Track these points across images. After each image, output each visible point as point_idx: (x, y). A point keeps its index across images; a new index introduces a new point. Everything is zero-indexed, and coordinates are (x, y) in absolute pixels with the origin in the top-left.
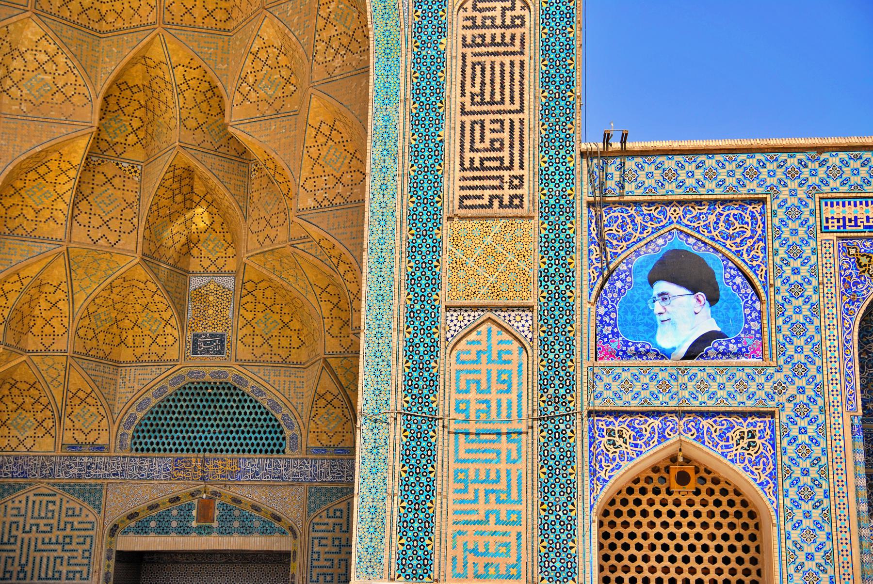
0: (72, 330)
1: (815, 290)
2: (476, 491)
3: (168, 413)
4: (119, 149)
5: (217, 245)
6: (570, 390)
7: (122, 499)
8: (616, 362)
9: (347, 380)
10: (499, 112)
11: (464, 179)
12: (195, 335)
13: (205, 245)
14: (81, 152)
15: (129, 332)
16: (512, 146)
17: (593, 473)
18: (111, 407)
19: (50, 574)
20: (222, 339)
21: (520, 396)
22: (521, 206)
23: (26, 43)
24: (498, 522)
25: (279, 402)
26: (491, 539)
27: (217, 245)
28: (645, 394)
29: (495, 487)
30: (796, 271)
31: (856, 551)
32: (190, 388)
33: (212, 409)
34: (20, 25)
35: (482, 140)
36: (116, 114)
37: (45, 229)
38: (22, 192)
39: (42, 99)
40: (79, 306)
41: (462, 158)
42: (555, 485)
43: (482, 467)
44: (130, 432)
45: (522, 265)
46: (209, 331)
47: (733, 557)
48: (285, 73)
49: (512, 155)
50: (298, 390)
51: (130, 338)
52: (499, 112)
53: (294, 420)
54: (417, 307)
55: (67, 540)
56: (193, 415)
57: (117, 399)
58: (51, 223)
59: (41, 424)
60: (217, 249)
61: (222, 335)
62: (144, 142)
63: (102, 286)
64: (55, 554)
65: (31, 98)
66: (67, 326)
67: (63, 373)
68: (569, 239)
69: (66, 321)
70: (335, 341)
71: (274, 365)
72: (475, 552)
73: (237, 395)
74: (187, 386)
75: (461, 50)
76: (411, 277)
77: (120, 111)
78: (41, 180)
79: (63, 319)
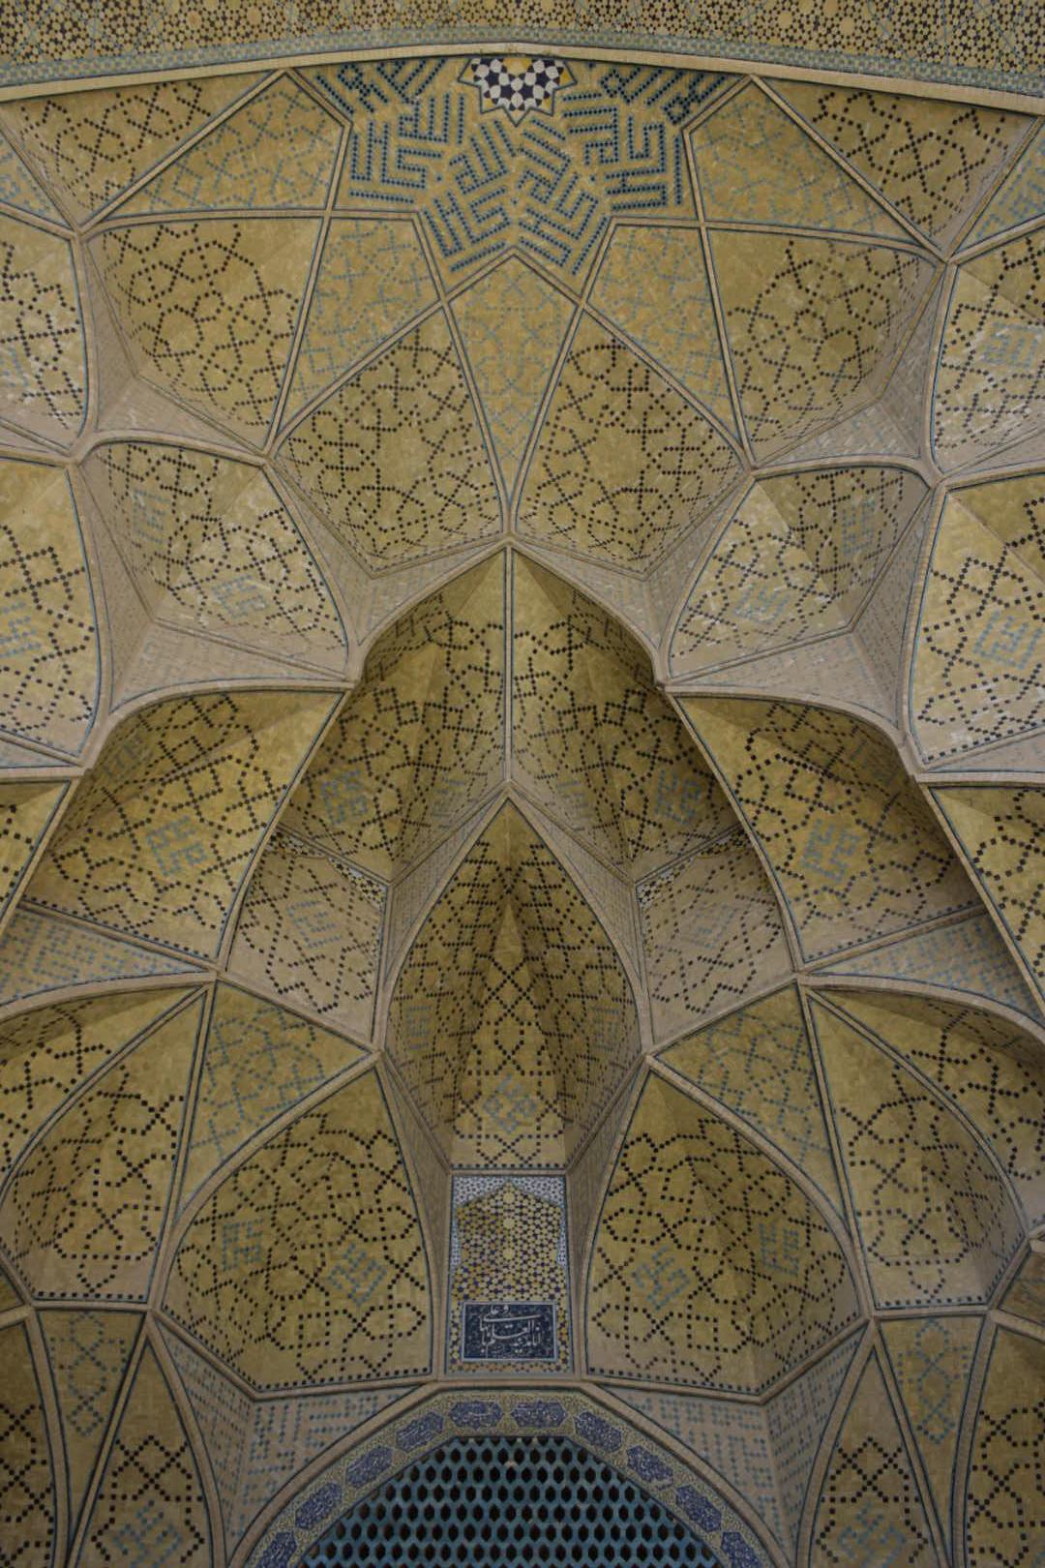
0: (168, 1247)
3: (389, 1533)
4: (346, 845)
5: (518, 1107)
9: (925, 1400)
12: (470, 1309)
13: (492, 1105)
14: (302, 749)
15: (290, 1306)
18: (226, 1511)
20: (543, 1317)
23: (240, 516)
25: (712, 1497)
27: (518, 1107)
32: (456, 1456)
33: (518, 1520)
34: (240, 474)
36: (353, 768)
37: (172, 928)
38: (139, 833)
39: (243, 619)
40: (194, 1187)
46: (509, 1300)
50: (755, 1462)
51: (292, 1323)
53: (758, 1551)
56: (461, 1540)
57: (241, 1493)
58: (190, 920)
60: (520, 1117)
61: (543, 1308)
62: (394, 848)
63: (266, 1134)
65: (224, 612)
66: (156, 1233)
67: (113, 1383)
69: (155, 1220)
73: (590, 1476)
74: (448, 1450)
77: (362, 764)
78: (190, 811)
79: (151, 1213)
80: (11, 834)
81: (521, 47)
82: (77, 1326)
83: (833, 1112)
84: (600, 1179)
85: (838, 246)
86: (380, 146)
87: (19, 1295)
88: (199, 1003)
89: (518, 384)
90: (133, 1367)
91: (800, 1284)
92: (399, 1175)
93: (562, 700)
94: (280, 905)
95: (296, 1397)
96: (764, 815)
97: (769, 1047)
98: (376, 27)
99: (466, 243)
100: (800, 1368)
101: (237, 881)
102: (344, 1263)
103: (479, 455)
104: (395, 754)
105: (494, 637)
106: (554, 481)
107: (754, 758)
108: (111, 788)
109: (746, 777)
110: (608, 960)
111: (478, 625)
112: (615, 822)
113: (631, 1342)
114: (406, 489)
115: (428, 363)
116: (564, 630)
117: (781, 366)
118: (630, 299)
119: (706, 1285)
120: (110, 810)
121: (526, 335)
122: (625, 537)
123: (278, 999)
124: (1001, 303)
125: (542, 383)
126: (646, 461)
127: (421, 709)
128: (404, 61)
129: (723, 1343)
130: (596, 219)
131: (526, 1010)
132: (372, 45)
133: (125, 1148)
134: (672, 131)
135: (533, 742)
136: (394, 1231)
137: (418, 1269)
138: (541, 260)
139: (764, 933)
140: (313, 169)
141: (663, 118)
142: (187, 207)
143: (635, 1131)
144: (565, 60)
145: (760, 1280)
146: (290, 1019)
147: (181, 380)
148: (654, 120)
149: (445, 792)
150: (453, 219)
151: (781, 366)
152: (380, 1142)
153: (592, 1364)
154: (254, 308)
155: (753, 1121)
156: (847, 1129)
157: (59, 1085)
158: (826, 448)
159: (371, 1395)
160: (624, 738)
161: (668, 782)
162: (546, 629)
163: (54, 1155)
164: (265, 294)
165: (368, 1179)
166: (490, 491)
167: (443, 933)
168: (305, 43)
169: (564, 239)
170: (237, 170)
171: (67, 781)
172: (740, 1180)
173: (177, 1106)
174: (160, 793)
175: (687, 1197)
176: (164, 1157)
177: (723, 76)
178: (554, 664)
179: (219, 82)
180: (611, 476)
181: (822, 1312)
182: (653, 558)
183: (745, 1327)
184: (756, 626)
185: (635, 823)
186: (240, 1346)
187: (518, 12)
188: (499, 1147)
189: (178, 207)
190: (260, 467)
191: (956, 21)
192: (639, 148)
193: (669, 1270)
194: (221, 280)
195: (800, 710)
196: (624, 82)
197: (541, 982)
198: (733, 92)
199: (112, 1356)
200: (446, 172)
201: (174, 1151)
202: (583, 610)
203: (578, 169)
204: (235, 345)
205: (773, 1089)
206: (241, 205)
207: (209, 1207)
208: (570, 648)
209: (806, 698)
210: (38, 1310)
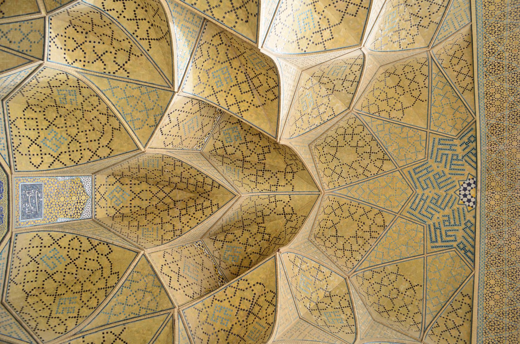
13: (118, 189)
14: (256, 123)
34: (347, 101)
36: (243, 138)
38: (227, 64)
39: (300, 102)
40: (92, 80)
46: (44, 200)
51: (34, 115)
60: (114, 200)
62: (214, 152)
63: (113, 108)
66: (75, 65)
67: (12, 46)
77: (244, 141)
78: (235, 82)
80: (237, 20)
81: (479, 193)
82: (37, 33)
83: (124, 324)
84: (93, 234)
85: (421, 302)
86: (449, 148)
87: (52, 11)
88: (166, 85)
89: (371, 194)
90: (20, 54)
91: (53, 315)
92: (95, 157)
93: (267, 212)
94: (198, 113)
95: (4, 117)
96: (234, 290)
97: (148, 298)
98: (487, 148)
99: (417, 176)
100: (19, 318)
101: (209, 99)
102: (59, 136)
103: (348, 181)
104: (248, 153)
107: (254, 285)
108: (245, 55)
109: (247, 282)
110: (177, 233)
111: (293, 182)
112: (223, 231)
113: (28, 249)
114: (336, 156)
115: (379, 163)
116: (291, 212)
117: (381, 284)
118: (400, 231)
119: (50, 276)
120: (236, 53)
121: (388, 196)
122: (321, 231)
123: (166, 114)
126: (347, 238)
127: (263, 162)
128: (476, 157)
129: (26, 284)
130: (425, 219)
131: (155, 201)
132: (482, 147)
133: (108, 54)
134: (455, 244)
135: (253, 202)
136: (72, 155)
137: (57, 165)
138: (412, 201)
139: (190, 292)
140: (443, 126)
141: (459, 241)
142: (433, 85)
143: (113, 247)
144: (476, 208)
145: (53, 298)
146: (158, 118)
147: (377, 81)
148: (458, 238)
149: (235, 171)
152: (109, 151)
153: (19, 235)
154: (398, 106)
155: (119, 293)
156: (117, 330)
157: (136, 31)
158: (358, 303)
159: (6, 148)
160: (253, 234)
161: (238, 250)
162: (292, 206)
163: (107, 27)
164: (403, 109)
165: (94, 146)
166: (337, 186)
167: (186, 172)
168: (483, 125)
169: (419, 208)
170: (444, 102)
171: (257, 42)
172: (94, 289)
173: (125, 74)
174: (242, 72)
175: (86, 268)
176: (105, 69)
177: (474, 261)
178: (279, 209)
179: (473, 97)
180: (341, 226)
181: (43, 325)
182: (316, 242)
183: (33, 293)
184: (299, 282)
185: (222, 238)
186: (26, 96)
187: (490, 193)
188: (102, 193)
189: (433, 82)
190: (349, 108)
191: (496, 339)
192: (449, 233)
193: (56, 262)
194: (408, 95)
195: (274, 303)
196: (469, 228)
197: (166, 207)
198: (469, 265)
199: (24, 46)
200: (440, 170)
201: (107, 73)
202: (299, 219)
203: (441, 213)
204: (387, 99)
205: (132, 300)
206: (432, 102)
207: (84, 85)
208: (285, 214)
209: (279, 305)
210: (45, 18)
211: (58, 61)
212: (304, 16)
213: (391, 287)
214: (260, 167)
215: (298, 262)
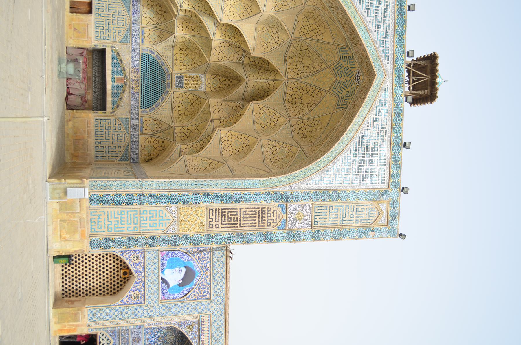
1: (182, 314)
2: (118, 218)
6: (151, 246)
7: (124, 51)
8: (160, 257)
10: (240, 220)
11: (219, 210)
16: (229, 224)
17: (125, 252)
19: (97, 25)
20: (181, 86)
21: (148, 230)
22: (210, 228)
24: (108, 225)
26: (103, 223)
28: (150, 267)
29: (119, 223)
30: (188, 309)
31: (104, 327)
35: (231, 215)
41: (226, 209)
42: (120, 242)
43: (125, 219)
44: (148, 52)
45: (190, 229)
47: (102, 288)
48: (268, 124)
49: (226, 224)
51: (182, 52)
52: (240, 220)
54: (177, 197)
55: (110, 31)
59: (152, 20)
64: (104, 26)
68: (198, 244)
70: (179, 131)
71: (172, 105)
72: (99, 218)
75: (261, 207)
76: (187, 195)
103: (306, 74)
105: (274, 78)
106: (302, 88)
115: (320, 65)
117: (310, 126)
122: (294, 100)
124: (290, 152)
125: (317, 85)
130: (339, 94)
134: (345, 106)
137: (188, 69)
139: (222, 116)
150: (340, 67)
151: (310, 126)
154: (319, 33)
164: (322, 34)
166: (299, 76)
178: (272, 88)
199: (171, 30)
211: (181, 33)
212: (238, 6)
213: (314, 128)
214: (266, 69)
215: (264, 109)
